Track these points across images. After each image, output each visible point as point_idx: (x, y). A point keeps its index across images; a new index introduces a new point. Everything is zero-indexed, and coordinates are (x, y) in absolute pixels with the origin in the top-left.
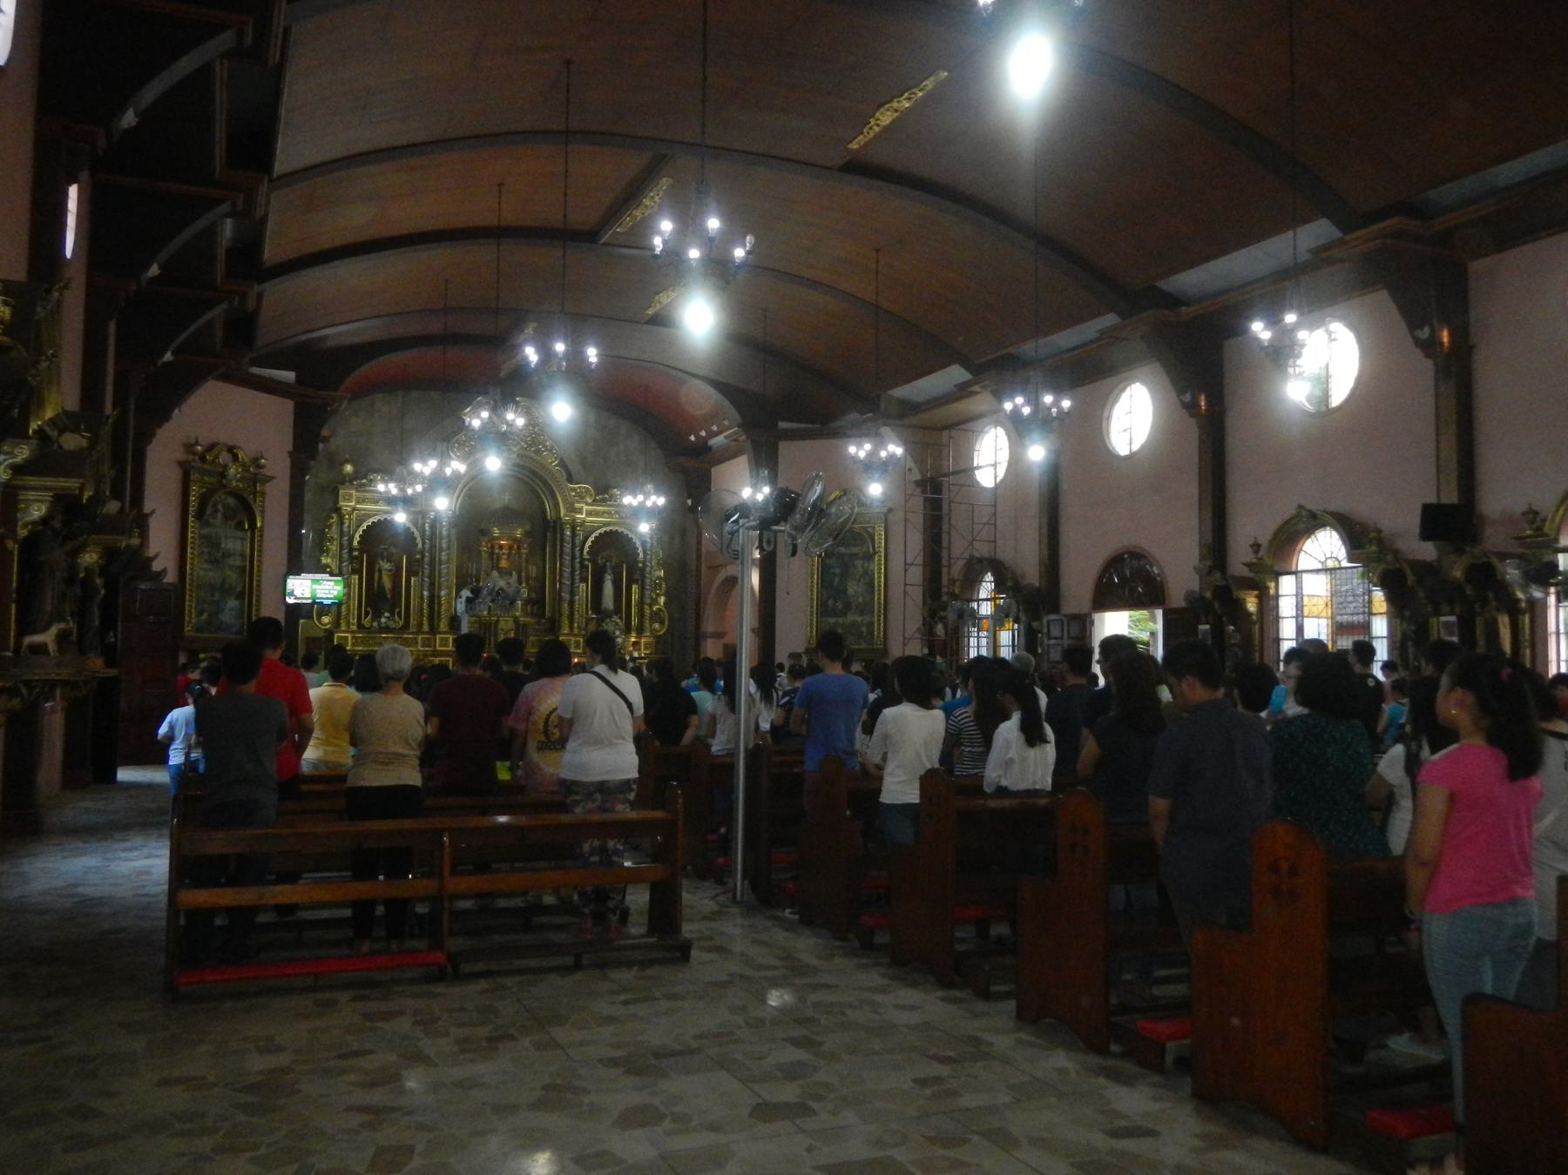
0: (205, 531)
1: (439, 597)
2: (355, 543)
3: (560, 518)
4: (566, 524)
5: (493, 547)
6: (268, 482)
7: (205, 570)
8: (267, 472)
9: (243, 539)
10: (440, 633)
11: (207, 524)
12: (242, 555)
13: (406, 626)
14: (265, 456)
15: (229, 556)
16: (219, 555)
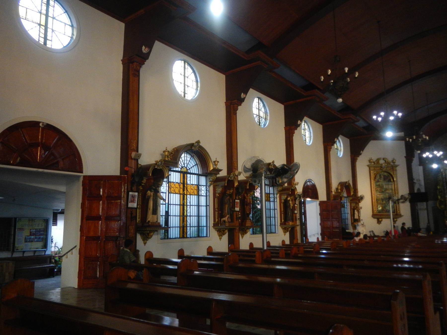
0: (378, 184)
7: (380, 195)
8: (396, 164)
11: (378, 181)
12: (392, 189)
14: (395, 159)
16: (383, 190)
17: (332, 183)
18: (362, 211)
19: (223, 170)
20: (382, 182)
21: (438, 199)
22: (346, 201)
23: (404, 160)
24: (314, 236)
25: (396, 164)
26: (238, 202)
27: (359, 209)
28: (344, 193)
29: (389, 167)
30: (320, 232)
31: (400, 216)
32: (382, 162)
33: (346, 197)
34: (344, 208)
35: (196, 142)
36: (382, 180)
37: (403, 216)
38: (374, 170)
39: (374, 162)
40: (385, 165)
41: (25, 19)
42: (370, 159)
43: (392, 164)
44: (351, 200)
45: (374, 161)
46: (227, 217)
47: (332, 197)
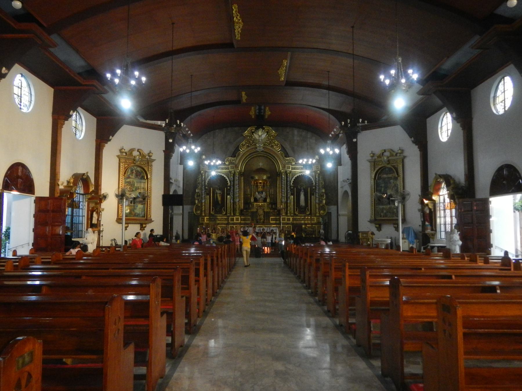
0: (128, 180)
1: (236, 203)
2: (206, 184)
3: (280, 171)
4: (283, 173)
5: (257, 183)
6: (153, 161)
8: (153, 158)
9: (144, 183)
10: (236, 216)
11: (129, 177)
13: (226, 214)
14: (152, 152)
15: (138, 189)
16: (134, 189)
17: (59, 173)
18: (104, 214)
20: (133, 179)
21: (195, 203)
22: (83, 200)
23: (163, 154)
24: (23, 247)
25: (153, 158)
27: (100, 212)
28: (81, 188)
29: (144, 160)
30: (31, 241)
31: (151, 221)
32: (135, 153)
33: (82, 194)
34: (78, 210)
36: (133, 177)
37: (153, 221)
38: (125, 162)
39: (126, 153)
40: (139, 158)
42: (121, 147)
43: (147, 157)
44: (89, 199)
45: (126, 151)
47: (58, 193)
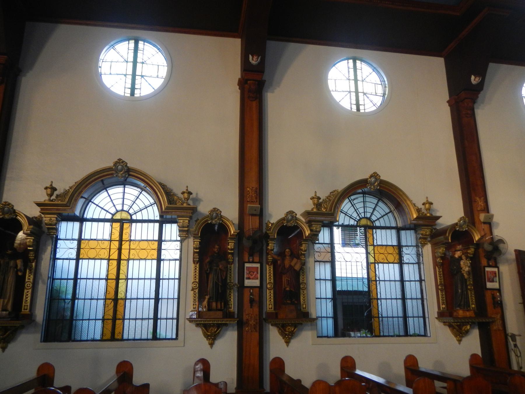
19: (441, 217)
26: (258, 268)
35: (371, 176)
41: (336, 91)
46: (206, 300)
